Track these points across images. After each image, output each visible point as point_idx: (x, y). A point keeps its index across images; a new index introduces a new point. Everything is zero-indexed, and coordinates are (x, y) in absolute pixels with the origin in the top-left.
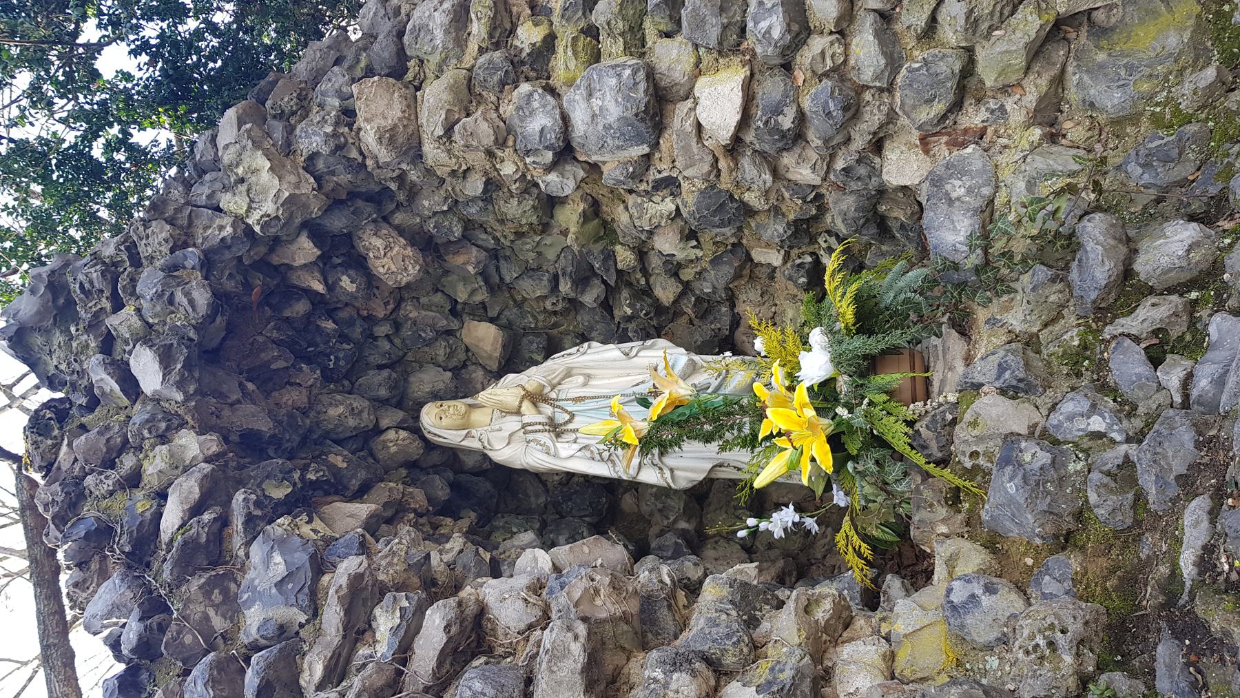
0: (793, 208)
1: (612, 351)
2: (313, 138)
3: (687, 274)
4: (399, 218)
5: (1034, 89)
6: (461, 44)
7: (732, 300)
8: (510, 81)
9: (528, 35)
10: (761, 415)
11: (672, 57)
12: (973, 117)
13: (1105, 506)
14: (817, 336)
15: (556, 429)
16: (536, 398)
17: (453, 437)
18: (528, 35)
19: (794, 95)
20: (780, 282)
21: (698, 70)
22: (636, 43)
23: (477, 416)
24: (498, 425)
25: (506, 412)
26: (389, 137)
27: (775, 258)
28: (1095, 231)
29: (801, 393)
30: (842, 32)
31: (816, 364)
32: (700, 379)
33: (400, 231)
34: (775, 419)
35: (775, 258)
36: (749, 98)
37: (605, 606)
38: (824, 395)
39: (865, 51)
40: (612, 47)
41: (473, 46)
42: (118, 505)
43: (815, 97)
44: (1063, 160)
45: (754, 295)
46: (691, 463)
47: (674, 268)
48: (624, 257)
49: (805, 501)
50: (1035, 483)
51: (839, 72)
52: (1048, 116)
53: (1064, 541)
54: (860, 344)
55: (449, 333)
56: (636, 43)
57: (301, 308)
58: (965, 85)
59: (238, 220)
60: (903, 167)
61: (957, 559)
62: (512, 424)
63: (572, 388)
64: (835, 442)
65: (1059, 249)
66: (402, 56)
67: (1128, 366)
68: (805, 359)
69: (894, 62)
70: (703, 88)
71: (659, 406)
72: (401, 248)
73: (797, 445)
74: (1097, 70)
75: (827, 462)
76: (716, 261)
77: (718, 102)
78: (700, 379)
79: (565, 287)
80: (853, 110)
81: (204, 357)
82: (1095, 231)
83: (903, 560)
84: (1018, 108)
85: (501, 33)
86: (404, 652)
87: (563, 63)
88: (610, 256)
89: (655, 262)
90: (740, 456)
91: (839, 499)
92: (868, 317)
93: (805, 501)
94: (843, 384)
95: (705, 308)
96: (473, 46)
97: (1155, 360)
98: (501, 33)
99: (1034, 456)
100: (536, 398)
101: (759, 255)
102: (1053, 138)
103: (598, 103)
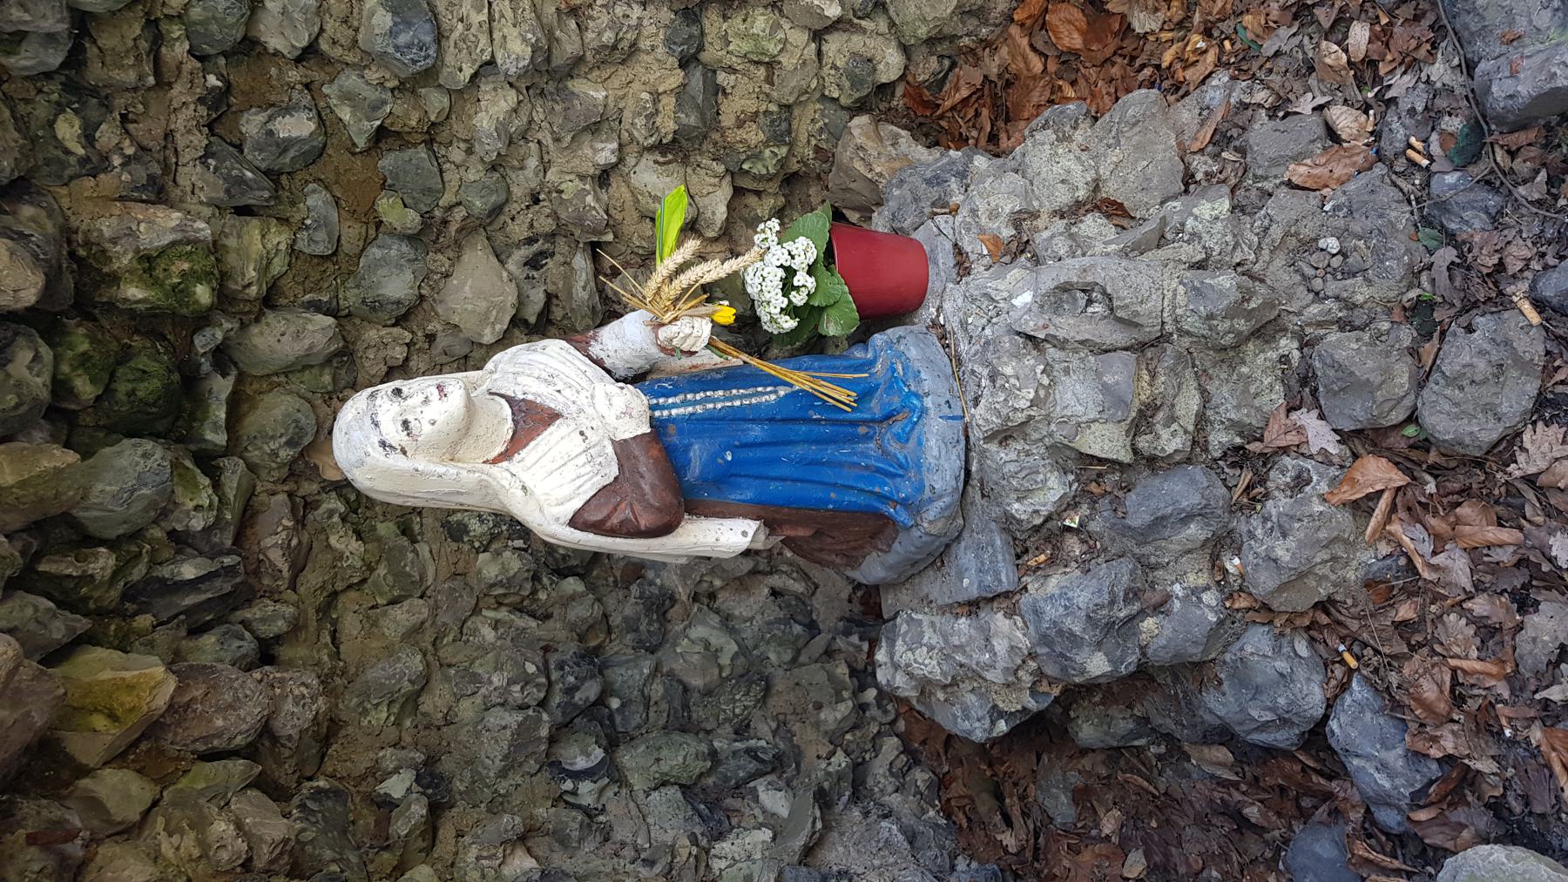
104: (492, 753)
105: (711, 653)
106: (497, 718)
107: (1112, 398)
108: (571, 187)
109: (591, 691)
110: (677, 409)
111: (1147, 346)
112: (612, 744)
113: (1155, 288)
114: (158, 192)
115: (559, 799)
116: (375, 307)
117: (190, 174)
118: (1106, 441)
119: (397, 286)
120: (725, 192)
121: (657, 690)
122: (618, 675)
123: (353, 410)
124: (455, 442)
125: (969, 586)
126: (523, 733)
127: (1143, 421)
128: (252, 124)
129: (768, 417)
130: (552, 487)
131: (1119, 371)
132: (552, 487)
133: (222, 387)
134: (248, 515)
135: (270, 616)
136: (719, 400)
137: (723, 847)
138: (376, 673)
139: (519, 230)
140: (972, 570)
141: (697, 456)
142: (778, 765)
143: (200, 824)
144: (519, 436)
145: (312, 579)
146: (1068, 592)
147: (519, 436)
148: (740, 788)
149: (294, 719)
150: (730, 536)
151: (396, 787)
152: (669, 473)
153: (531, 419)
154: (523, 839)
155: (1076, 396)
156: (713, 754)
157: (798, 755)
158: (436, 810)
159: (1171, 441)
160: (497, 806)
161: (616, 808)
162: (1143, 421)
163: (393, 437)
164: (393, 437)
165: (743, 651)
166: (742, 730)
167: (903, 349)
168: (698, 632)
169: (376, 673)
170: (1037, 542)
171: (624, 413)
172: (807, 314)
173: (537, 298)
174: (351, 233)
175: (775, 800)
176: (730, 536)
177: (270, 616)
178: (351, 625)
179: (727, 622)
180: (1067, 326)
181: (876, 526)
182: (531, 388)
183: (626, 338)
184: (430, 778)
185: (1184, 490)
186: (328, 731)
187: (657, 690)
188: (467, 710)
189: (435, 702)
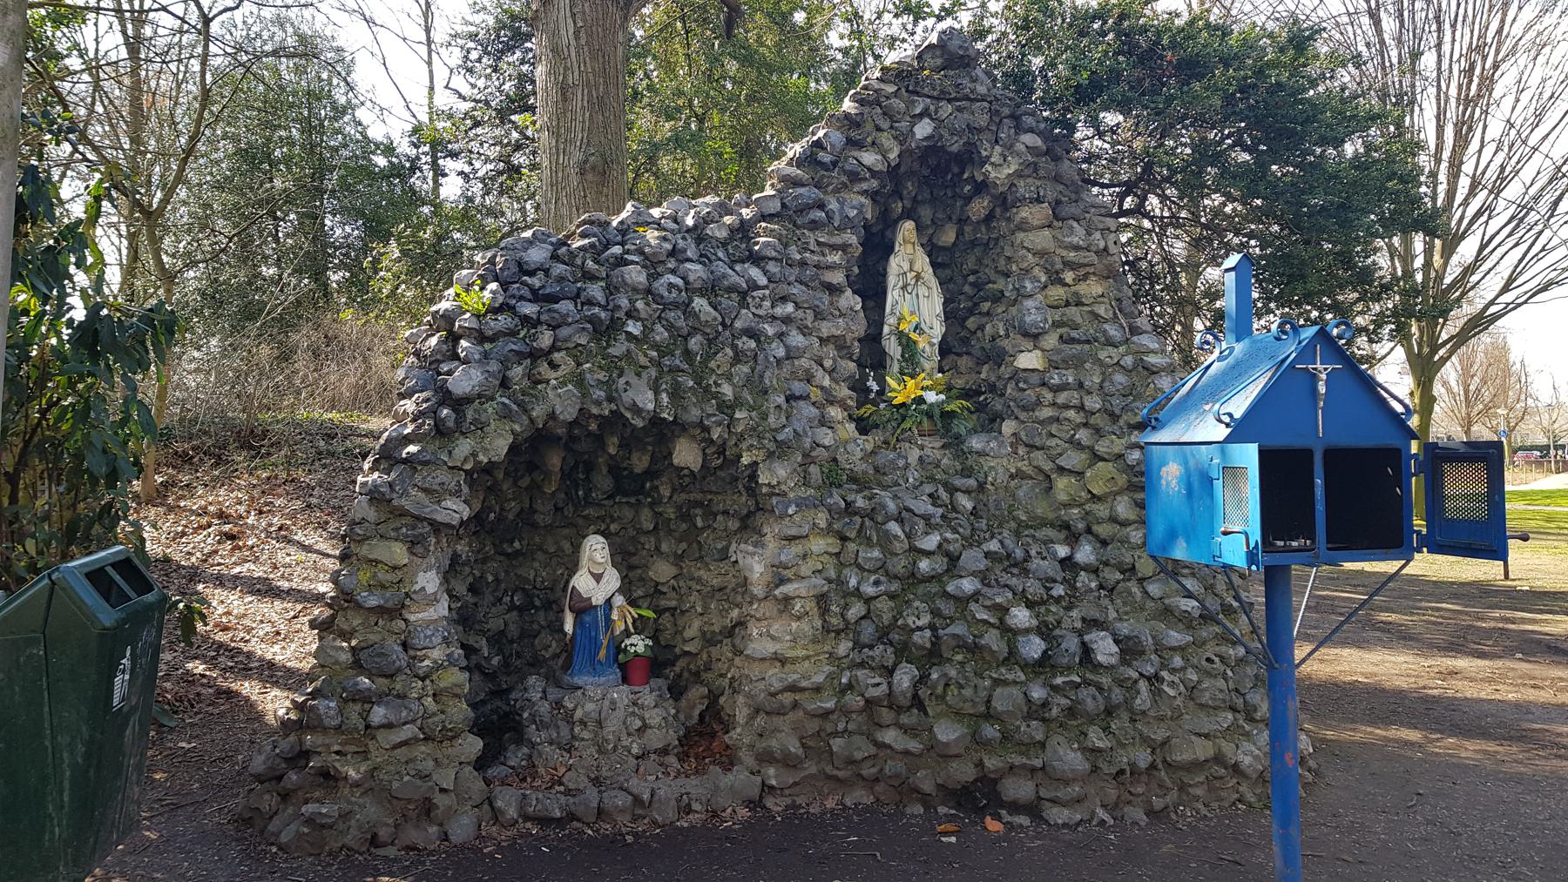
0: (1000, 385)
1: (939, 309)
2: (1024, 188)
3: (979, 333)
4: (998, 210)
5: (1029, 471)
6: (1066, 248)
7: (968, 353)
8: (1047, 271)
9: (1069, 276)
10: (912, 377)
11: (1051, 341)
12: (1021, 451)
13: (888, 479)
14: (942, 397)
15: (904, 288)
16: (918, 277)
17: (900, 238)
18: (1069, 276)
19: (1032, 387)
20: (974, 376)
21: (1043, 350)
22: (1056, 325)
23: (910, 246)
24: (907, 259)
25: (912, 264)
26: (1024, 221)
27: (983, 376)
28: (972, 482)
29: (920, 393)
30: (1054, 404)
31: (931, 397)
32: (928, 349)
33: (992, 211)
34: (911, 383)
35: (983, 376)
36: (1033, 370)
37: (849, 337)
38: (920, 400)
39: (1046, 413)
40: (1058, 315)
41: (1064, 253)
42: (869, 127)
43: (1030, 394)
44: (1002, 478)
45: (970, 364)
46: (892, 347)
47: (982, 328)
48: (986, 306)
49: (881, 393)
50: (892, 462)
51: (1039, 403)
52: (1019, 475)
53: (877, 470)
54: (937, 412)
55: (950, 218)
56: (1056, 325)
57: (956, 170)
58: (1032, 447)
59: (988, 157)
60: (1008, 427)
61: (868, 442)
62: (906, 267)
63: (922, 291)
64: (903, 405)
65: (967, 472)
66: (1063, 220)
67: (929, 488)
68: (933, 393)
69: (1041, 423)
70: (1038, 352)
71: (914, 336)
72: (983, 213)
73: (902, 390)
74: (1033, 488)
75: (895, 402)
76: (983, 349)
77: (1029, 360)
78: (928, 349)
79: (971, 279)
80: (1024, 408)
81: (932, 148)
82: (972, 482)
83: (864, 427)
84: (1024, 466)
85: (1069, 265)
86: (828, 268)
87: (1057, 292)
88: (986, 300)
89: (985, 320)
90: (896, 368)
91: (882, 406)
92: (948, 416)
93: (881, 393)
94: (924, 407)
95: (965, 341)
96: (1064, 253)
97: (930, 495)
98: (1069, 265)
99: (901, 463)
100: (918, 277)
101: (986, 367)
102: (1012, 477)
103: (1033, 312)
104: (521, 572)
105: (547, 647)
106: (532, 573)
107: (587, 714)
108: (692, 599)
109: (537, 603)
110: (600, 613)
111: (600, 723)
112: (520, 609)
113: (612, 727)
114: (674, 490)
115: (506, 591)
116: (659, 541)
117: (684, 496)
118: (579, 714)
119: (664, 547)
120: (694, 651)
121: (535, 626)
122: (542, 613)
123: (601, 539)
124: (591, 559)
125: (550, 690)
126: (527, 581)
127: (583, 723)
128: (698, 511)
129: (596, 638)
130: (582, 582)
131: (594, 715)
132: (582, 582)
133: (633, 500)
134: (599, 505)
135: (569, 511)
136: (602, 624)
137: (484, 641)
138: (550, 540)
139: (682, 583)
140: (554, 693)
141: (587, 618)
142: (506, 663)
143: (514, 499)
144: (596, 576)
145: (580, 521)
146: (544, 708)
147: (596, 576)
148: (500, 652)
149: (539, 518)
150: (569, 627)
151: (517, 544)
152: (583, 609)
153: (598, 578)
154: (497, 580)
155: (590, 706)
156: (512, 642)
157: (509, 674)
158: (508, 555)
159: (577, 730)
160: (507, 572)
161: (501, 608)
162: (583, 723)
163: (596, 548)
164: (596, 548)
165: (546, 660)
166: (519, 655)
167: (615, 674)
168: (554, 644)
169: (550, 540)
170: (558, 704)
171: (598, 599)
172: (625, 651)
173: (664, 589)
174: (677, 535)
175: (495, 661)
176: (569, 627)
177: (569, 511)
178: (566, 531)
179: (556, 656)
180: (607, 703)
181: (567, 667)
182: (604, 580)
183: (619, 600)
184: (517, 553)
185: (565, 732)
186: (535, 526)
187: (535, 626)
188: (536, 565)
189: (540, 556)
